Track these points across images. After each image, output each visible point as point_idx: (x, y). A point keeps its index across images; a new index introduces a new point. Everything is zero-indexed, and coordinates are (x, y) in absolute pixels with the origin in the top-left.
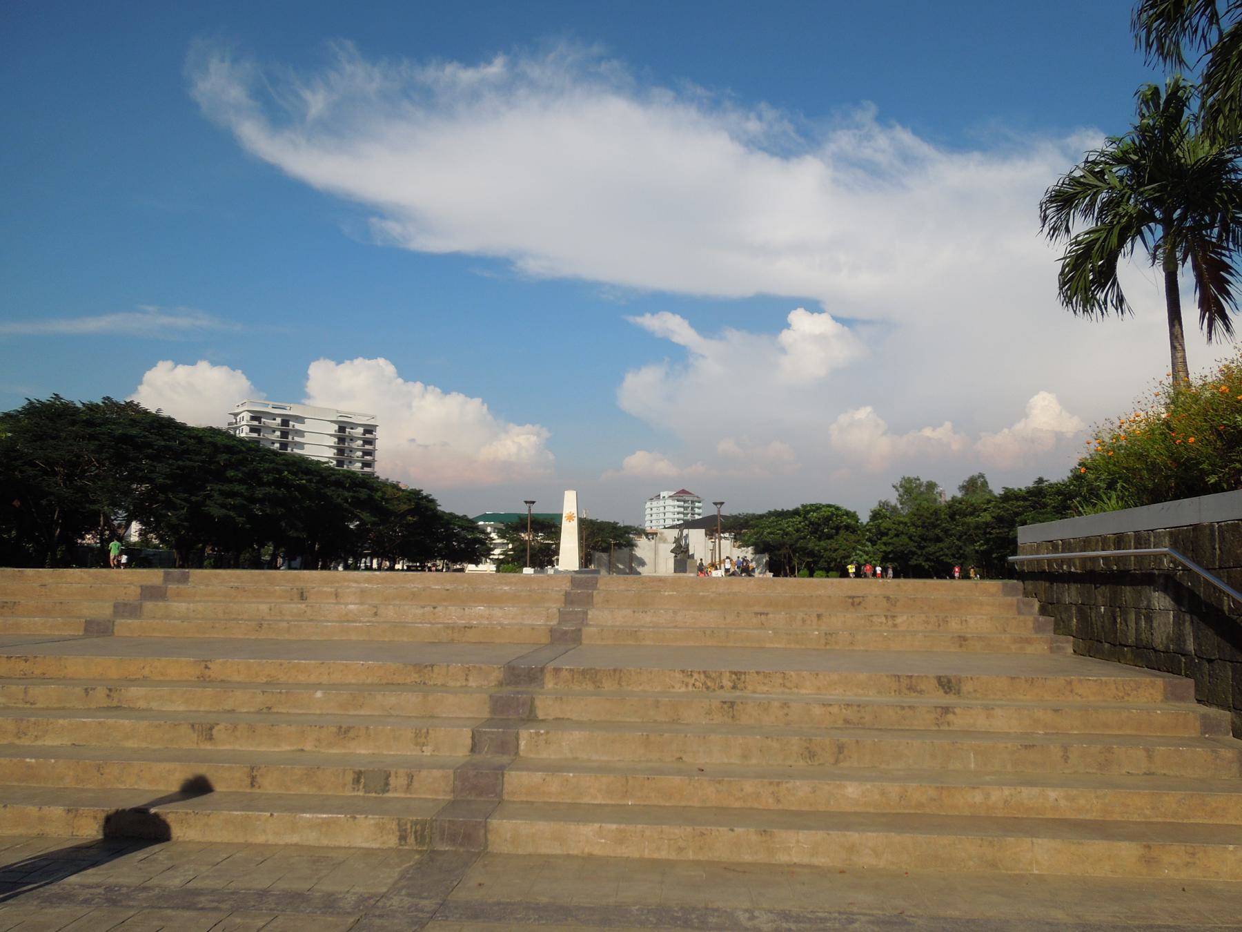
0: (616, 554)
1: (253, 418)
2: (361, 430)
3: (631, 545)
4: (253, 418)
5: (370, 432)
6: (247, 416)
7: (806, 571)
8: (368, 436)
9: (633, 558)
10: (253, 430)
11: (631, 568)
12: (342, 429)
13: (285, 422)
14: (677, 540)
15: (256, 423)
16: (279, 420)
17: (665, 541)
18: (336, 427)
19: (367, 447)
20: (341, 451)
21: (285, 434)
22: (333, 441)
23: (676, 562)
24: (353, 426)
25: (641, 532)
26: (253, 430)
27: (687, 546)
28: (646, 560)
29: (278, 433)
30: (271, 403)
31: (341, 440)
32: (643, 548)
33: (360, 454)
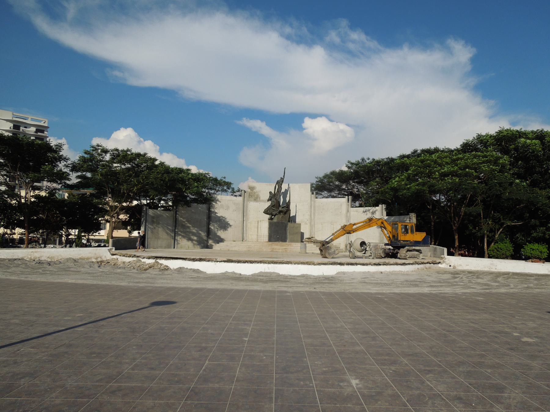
0: (183, 213)
2: (33, 129)
3: (208, 201)
5: (42, 131)
7: (507, 246)
8: (39, 134)
9: (210, 217)
11: (209, 232)
14: (273, 197)
17: (256, 199)
18: (12, 125)
23: (272, 226)
24: (27, 126)
25: (224, 186)
27: (288, 205)
28: (231, 223)
32: (225, 205)
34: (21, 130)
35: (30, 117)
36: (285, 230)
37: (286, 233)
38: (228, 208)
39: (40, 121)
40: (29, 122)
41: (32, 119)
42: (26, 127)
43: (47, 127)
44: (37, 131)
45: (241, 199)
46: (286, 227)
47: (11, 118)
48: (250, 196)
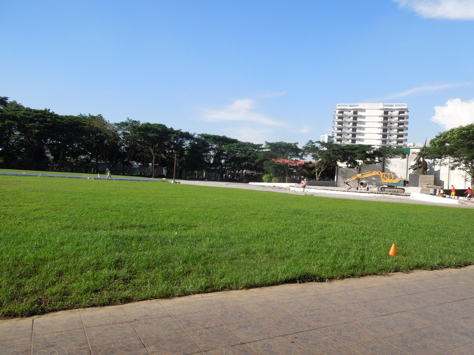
1: (339, 112)
2: (397, 112)
4: (339, 112)
5: (403, 112)
6: (337, 111)
8: (401, 115)
10: (340, 118)
12: (386, 113)
13: (355, 113)
15: (341, 114)
16: (352, 112)
18: (383, 112)
19: (401, 121)
20: (385, 124)
21: (355, 118)
22: (381, 119)
26: (340, 118)
29: (352, 118)
30: (348, 104)
31: (386, 118)
33: (396, 124)
34: (389, 114)
35: (395, 104)
36: (418, 179)
37: (418, 181)
38: (396, 166)
39: (403, 105)
40: (394, 108)
41: (396, 105)
42: (392, 112)
43: (407, 109)
44: (400, 113)
45: (405, 160)
46: (418, 177)
47: (382, 108)
48: (412, 158)
